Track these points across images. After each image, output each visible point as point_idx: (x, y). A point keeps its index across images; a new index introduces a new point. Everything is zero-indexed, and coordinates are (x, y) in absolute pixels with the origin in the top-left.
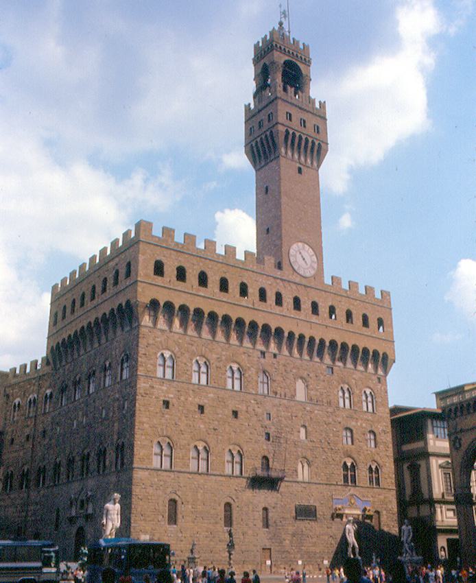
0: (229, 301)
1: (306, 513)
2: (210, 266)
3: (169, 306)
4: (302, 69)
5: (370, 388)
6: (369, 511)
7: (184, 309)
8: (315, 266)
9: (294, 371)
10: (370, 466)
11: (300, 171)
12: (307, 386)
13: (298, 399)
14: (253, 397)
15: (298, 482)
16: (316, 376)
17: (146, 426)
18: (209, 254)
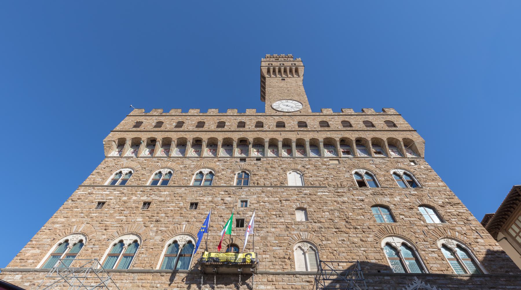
5: (401, 169)
13: (289, 185)
14: (224, 189)
15: (294, 274)
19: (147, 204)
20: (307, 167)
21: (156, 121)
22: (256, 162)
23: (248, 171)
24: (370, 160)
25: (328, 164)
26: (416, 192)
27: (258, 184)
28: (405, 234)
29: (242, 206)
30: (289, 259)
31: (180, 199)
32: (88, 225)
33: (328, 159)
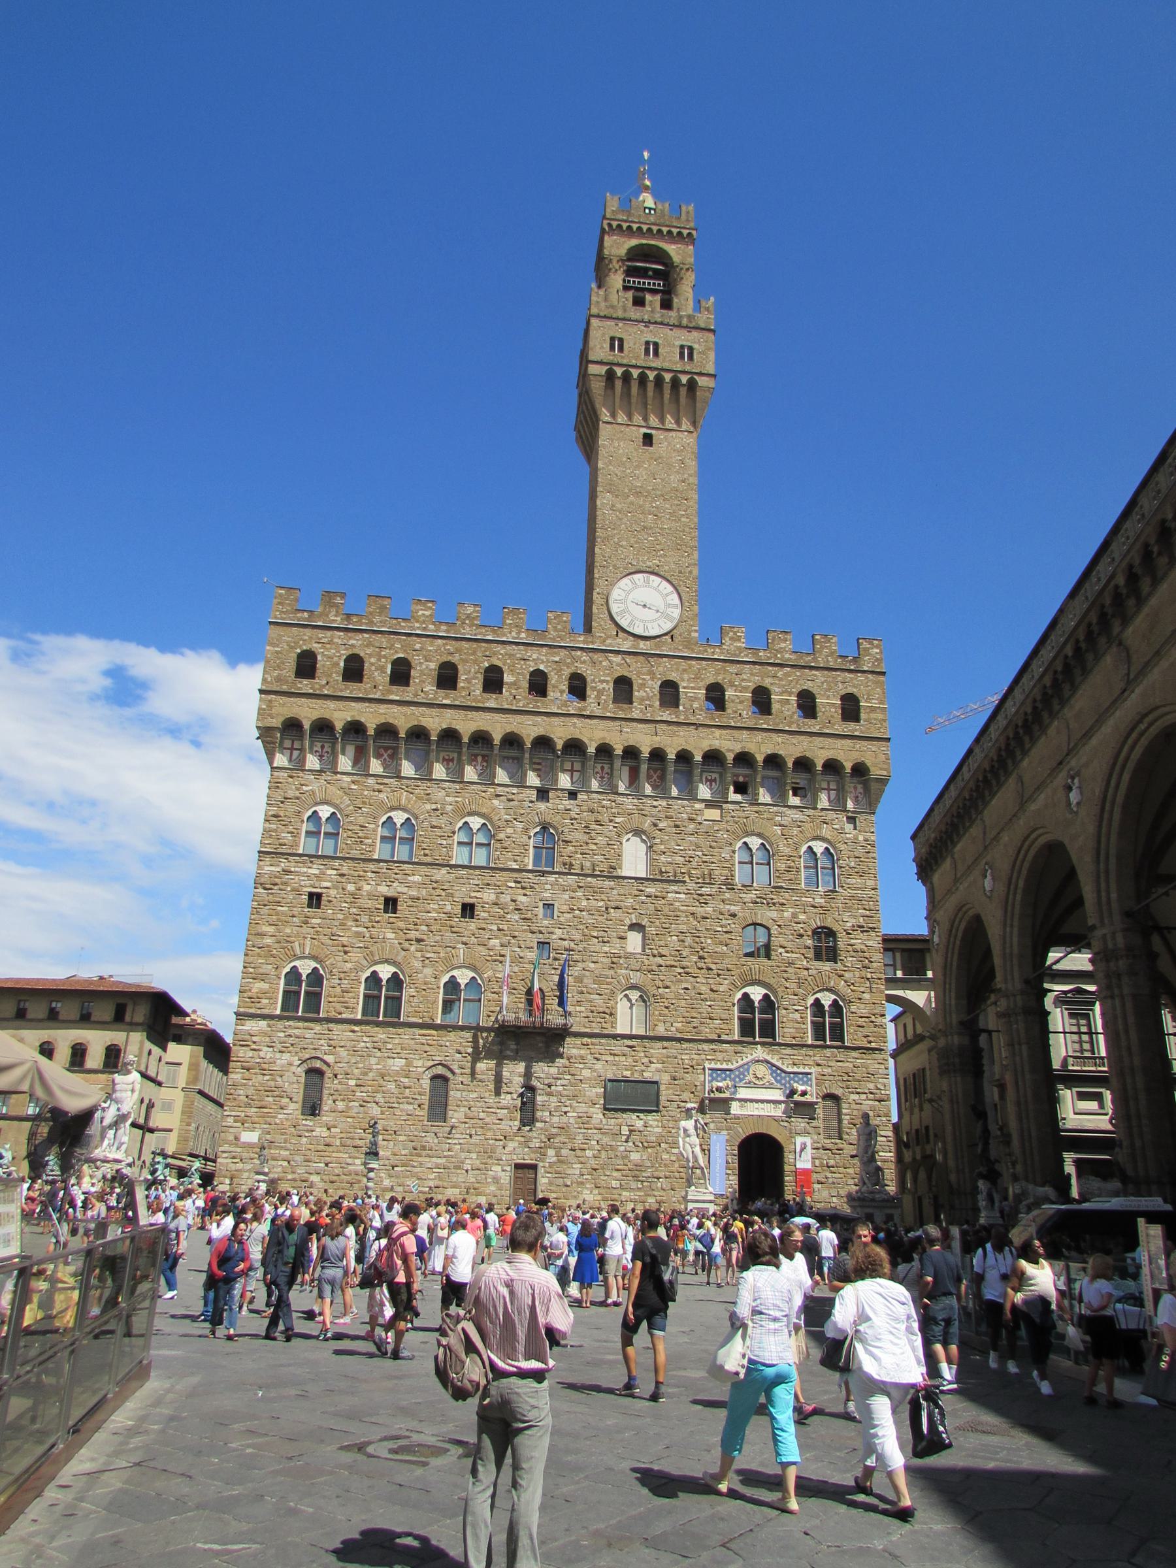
0: (457, 703)
1: (631, 1096)
2: (418, 646)
3: (323, 727)
4: (672, 254)
5: (823, 839)
6: (804, 1093)
7: (355, 729)
8: (676, 613)
9: (617, 820)
10: (817, 1001)
11: (648, 440)
12: (651, 847)
13: (626, 871)
14: (515, 875)
15: (615, 1037)
16: (677, 826)
17: (268, 941)
18: (417, 625)
19: (391, 904)
20: (661, 825)
21: (345, 653)
22: (568, 803)
23: (555, 828)
24: (776, 814)
25: (699, 818)
26: (822, 901)
27: (571, 865)
28: (772, 981)
29: (545, 916)
30: (611, 1014)
31: (443, 894)
32: (316, 942)
33: (703, 805)
